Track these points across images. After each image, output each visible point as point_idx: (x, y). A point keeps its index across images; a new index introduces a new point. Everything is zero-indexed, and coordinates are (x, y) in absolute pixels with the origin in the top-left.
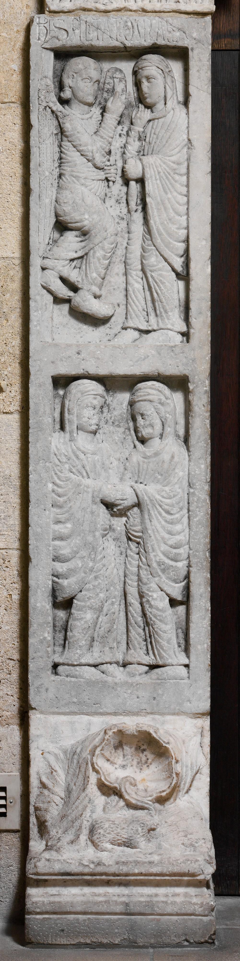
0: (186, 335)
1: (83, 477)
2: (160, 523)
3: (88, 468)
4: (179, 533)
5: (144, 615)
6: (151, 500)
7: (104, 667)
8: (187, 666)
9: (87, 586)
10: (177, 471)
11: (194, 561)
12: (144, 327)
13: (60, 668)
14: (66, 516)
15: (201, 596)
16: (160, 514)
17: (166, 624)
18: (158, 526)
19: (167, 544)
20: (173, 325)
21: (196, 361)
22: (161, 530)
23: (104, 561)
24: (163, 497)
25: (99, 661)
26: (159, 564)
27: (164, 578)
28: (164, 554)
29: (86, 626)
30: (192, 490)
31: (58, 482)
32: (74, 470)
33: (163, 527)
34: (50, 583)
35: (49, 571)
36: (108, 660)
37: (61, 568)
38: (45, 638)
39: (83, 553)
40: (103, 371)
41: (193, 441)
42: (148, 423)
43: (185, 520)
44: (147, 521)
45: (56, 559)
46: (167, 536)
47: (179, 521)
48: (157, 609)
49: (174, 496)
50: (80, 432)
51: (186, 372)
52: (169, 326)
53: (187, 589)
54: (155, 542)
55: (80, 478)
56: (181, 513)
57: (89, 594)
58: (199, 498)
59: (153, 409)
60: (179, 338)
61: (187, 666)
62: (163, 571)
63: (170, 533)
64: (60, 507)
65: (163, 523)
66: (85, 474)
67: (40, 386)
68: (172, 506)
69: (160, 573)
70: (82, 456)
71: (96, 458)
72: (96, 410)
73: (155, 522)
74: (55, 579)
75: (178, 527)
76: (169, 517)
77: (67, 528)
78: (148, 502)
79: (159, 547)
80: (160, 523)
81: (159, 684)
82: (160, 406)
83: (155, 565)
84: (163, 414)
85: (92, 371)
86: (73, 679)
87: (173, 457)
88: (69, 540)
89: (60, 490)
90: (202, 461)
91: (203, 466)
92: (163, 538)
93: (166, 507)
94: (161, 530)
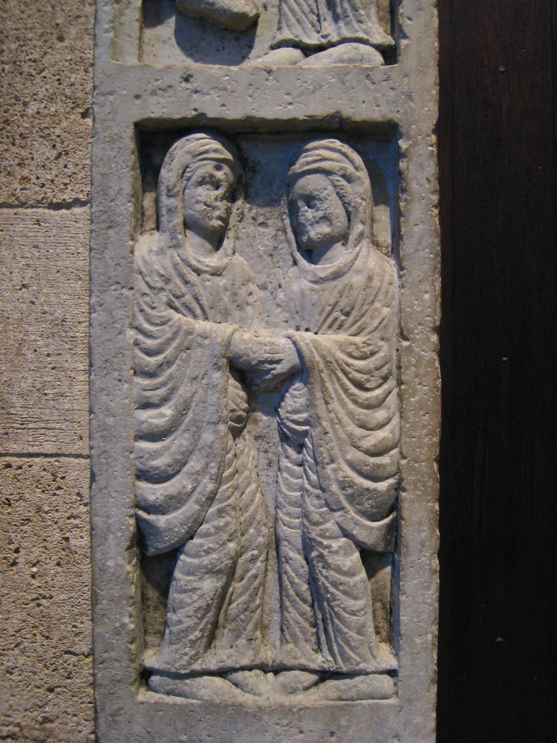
0: (390, 54)
1: (195, 317)
2: (344, 405)
3: (204, 301)
4: (381, 426)
5: (313, 581)
6: (327, 363)
7: (238, 676)
8: (392, 673)
9: (204, 527)
10: (377, 305)
11: (409, 478)
12: (313, 40)
13: (155, 679)
14: (161, 392)
15: (423, 544)
16: (346, 391)
17: (355, 598)
18: (342, 413)
19: (358, 448)
20: (366, 32)
21: (412, 99)
22: (346, 419)
23: (239, 479)
24: (350, 355)
25: (230, 663)
26: (344, 485)
27: (352, 513)
28: (352, 465)
29: (202, 603)
30: (406, 344)
31: (146, 326)
32: (177, 303)
33: (350, 414)
34: (132, 521)
35: (128, 500)
36: (245, 662)
37: (153, 492)
38: (124, 625)
39: (195, 464)
40: (234, 112)
41: (407, 247)
42: (320, 214)
43: (392, 400)
44: (320, 402)
45: (142, 475)
46: (359, 432)
47: (379, 404)
48: (338, 570)
49: (373, 354)
50: (189, 233)
51: (396, 117)
52: (361, 35)
53: (394, 529)
54: (334, 443)
55: (190, 319)
56: (385, 386)
57: (208, 543)
58: (420, 359)
59: (330, 188)
60: (379, 58)
61: (392, 673)
62: (351, 499)
63: (363, 426)
64: (151, 375)
65: (351, 406)
66: (198, 311)
67: (112, 141)
68: (369, 372)
69: (345, 504)
70: (193, 277)
71: (221, 282)
72: (220, 192)
73: (335, 405)
74: (143, 514)
75: (380, 415)
76: (363, 395)
77: (162, 415)
78: (322, 366)
79: (344, 453)
80: (344, 405)
81: (342, 708)
82: (343, 182)
83: (334, 488)
84: (350, 197)
85: (213, 111)
86: (179, 700)
87: (370, 278)
88: (168, 441)
89: (149, 343)
90: (426, 286)
91: (427, 296)
92: (350, 435)
93: (358, 376)
94: (346, 419)
